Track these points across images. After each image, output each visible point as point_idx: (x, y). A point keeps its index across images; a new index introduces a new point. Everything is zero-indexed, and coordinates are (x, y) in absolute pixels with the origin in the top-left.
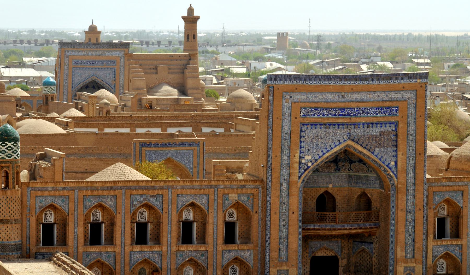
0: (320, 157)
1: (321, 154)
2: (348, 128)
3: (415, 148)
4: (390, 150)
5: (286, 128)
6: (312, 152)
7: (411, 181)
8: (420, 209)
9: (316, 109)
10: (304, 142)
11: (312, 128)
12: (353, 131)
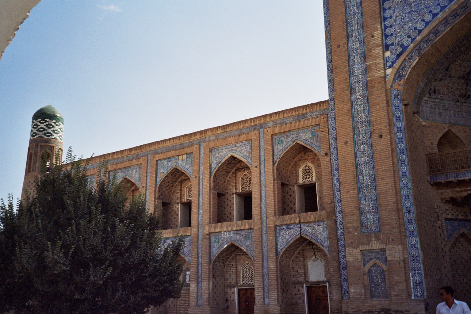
6: (410, 20)
10: (390, 8)
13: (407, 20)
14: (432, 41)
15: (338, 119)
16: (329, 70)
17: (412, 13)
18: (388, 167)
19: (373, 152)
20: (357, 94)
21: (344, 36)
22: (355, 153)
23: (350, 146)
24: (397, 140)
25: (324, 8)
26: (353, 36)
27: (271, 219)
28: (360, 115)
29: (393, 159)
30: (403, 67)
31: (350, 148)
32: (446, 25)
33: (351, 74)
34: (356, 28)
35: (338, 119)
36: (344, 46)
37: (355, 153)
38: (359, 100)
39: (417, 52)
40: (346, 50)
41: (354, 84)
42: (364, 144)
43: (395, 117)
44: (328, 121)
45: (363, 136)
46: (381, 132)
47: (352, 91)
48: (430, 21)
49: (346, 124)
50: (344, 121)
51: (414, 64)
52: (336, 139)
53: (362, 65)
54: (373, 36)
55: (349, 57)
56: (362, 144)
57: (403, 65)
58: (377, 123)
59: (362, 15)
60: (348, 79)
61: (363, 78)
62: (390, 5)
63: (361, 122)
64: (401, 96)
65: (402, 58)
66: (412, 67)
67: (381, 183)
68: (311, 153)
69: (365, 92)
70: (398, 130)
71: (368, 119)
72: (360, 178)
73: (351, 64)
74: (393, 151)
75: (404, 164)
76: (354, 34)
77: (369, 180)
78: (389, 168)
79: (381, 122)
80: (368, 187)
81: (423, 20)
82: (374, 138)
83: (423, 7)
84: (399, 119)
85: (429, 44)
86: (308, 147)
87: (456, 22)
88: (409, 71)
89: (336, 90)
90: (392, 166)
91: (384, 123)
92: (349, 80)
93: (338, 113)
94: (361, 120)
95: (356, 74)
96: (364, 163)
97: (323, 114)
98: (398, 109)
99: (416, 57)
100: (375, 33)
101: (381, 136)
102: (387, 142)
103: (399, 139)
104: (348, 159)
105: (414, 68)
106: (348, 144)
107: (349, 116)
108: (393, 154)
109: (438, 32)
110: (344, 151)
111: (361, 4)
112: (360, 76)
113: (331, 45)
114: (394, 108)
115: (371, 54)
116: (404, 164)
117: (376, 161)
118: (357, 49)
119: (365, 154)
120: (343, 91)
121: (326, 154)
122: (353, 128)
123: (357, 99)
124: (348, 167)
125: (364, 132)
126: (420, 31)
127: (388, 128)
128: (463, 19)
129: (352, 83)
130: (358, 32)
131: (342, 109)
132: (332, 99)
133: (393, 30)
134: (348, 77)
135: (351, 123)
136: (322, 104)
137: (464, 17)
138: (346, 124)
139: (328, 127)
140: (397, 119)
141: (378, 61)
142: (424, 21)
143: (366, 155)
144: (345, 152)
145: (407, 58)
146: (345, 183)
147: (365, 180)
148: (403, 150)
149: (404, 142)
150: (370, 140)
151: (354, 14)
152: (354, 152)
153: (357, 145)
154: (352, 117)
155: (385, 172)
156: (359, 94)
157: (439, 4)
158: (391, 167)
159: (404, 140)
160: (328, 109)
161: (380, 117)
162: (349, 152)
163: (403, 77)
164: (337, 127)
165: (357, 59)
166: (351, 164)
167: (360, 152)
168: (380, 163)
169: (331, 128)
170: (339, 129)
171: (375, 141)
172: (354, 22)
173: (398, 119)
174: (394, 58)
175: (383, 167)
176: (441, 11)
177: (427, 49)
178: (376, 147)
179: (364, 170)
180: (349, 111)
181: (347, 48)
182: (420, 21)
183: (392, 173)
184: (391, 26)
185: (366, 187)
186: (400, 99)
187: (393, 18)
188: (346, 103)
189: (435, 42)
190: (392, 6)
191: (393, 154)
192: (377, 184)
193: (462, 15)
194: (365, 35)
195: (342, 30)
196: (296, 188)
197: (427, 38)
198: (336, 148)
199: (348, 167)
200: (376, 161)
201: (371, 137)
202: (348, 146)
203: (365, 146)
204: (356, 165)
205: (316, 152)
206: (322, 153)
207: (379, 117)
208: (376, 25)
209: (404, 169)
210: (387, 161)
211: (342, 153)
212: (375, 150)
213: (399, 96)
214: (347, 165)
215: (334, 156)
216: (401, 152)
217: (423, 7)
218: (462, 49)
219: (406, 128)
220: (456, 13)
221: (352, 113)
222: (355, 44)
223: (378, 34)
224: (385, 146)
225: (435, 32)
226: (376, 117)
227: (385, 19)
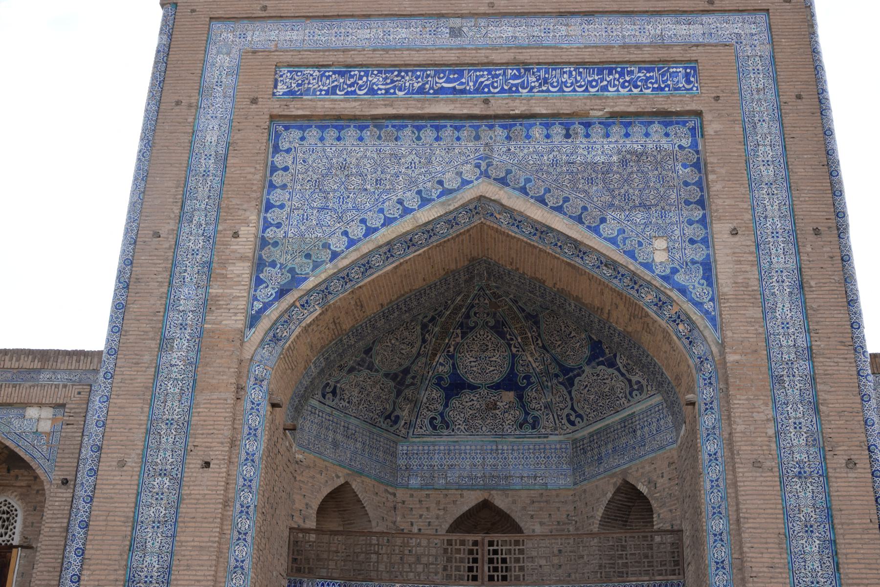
0: (352, 243)
1: (357, 231)
2: (477, 138)
3: (792, 210)
4: (673, 217)
5: (212, 137)
7: (788, 343)
8: (851, 464)
9: (341, 74)
10: (284, 187)
11: (322, 139)
13: (314, 222)
14: (352, 283)
15: (115, 401)
16: (122, 280)
17: (326, 211)
18: (207, 542)
19: (180, 499)
20: (174, 355)
21: (172, 216)
22: (138, 494)
23: (131, 473)
24: (241, 482)
25: (142, 140)
26: (192, 222)
28: (169, 403)
29: (222, 524)
30: (286, 318)
31: (129, 478)
32: (388, 258)
33: (169, 304)
34: (203, 206)
35: (115, 401)
36: (167, 238)
37: (138, 494)
38: (174, 369)
39: (320, 295)
40: (170, 248)
41: (173, 330)
42: (165, 474)
43: (246, 427)
44: (88, 401)
45: (165, 457)
46: (209, 455)
47: (164, 344)
48: (359, 240)
49: (132, 418)
50: (130, 409)
51: (309, 320)
52: (100, 448)
53: (200, 291)
54: (236, 235)
55: (174, 265)
56: (160, 475)
57: (286, 316)
58: (205, 432)
59: (222, 182)
60: (162, 314)
61: (195, 322)
62: (285, 182)
63: (169, 423)
64: (269, 384)
65: (289, 299)
66: (303, 324)
67: (182, 577)
68: (26, 473)
69: (192, 354)
70: (247, 459)
71: (186, 419)
72: (137, 555)
73: (176, 281)
74: (226, 504)
75: (245, 540)
76: (196, 218)
77: (157, 566)
78: (209, 544)
79: (216, 432)
80: (151, 582)
82: (191, 466)
83: (350, 205)
84: (255, 435)
85: (348, 286)
86: (22, 454)
87: (408, 258)
88: (296, 333)
89: (126, 331)
90: (217, 539)
91: (220, 436)
92: (164, 316)
93: (120, 387)
94: (170, 418)
95: (181, 308)
96: (154, 522)
97: (80, 382)
98: (257, 410)
99: (317, 307)
100: (242, 228)
101: (207, 464)
102: (218, 481)
103: (245, 480)
104: (117, 505)
105: (306, 329)
106: (125, 468)
107: (144, 399)
108: (225, 513)
109: (370, 267)
110: (113, 482)
111: (226, 159)
112: (190, 314)
113: (138, 226)
114: (249, 406)
115: (224, 272)
116: (245, 540)
117: (184, 522)
118: (195, 253)
119: (162, 499)
120: (144, 339)
121: (65, 482)
122: (148, 432)
123: (172, 365)
124: (113, 523)
125: (169, 447)
126: (335, 255)
127: (227, 449)
128: (420, 255)
129: (168, 326)
130: (206, 216)
131: (131, 380)
132: (112, 350)
133: (280, 234)
134: (162, 310)
135: (146, 418)
136: (82, 358)
137: (424, 252)
138: (132, 418)
139: (85, 416)
140: (250, 434)
141: (236, 293)
142: (347, 236)
143: (163, 502)
144: (114, 485)
145: (298, 304)
146: (97, 564)
147: (146, 564)
148: (248, 507)
149: (254, 489)
150: (180, 469)
151: (206, 174)
152: (137, 490)
153: (146, 475)
154: (151, 406)
155: (197, 553)
156: (179, 354)
157: (381, 211)
158: (215, 542)
159: (254, 484)
160: (96, 371)
161: (215, 419)
162: (123, 487)
163: (281, 343)
164: (108, 422)
165: (190, 271)
166: (123, 519)
167: (150, 492)
168: (191, 529)
169: (92, 419)
170: (114, 426)
171: (190, 474)
172: (203, 192)
173: (253, 433)
174: (272, 295)
175: (196, 539)
176: (383, 225)
177: (341, 296)
178: (192, 488)
179: (149, 539)
180: (146, 388)
181: (173, 243)
183: (214, 557)
184: (278, 226)
185: (146, 582)
186: (265, 387)
187: (286, 208)
188: (144, 369)
189: (360, 287)
190: (289, 185)
191: (225, 513)
192: (173, 577)
193: (421, 246)
194: (220, 228)
195: (171, 200)
197: (346, 272)
198: (94, 472)
199: (113, 523)
200: (184, 522)
202: (123, 473)
203: (166, 481)
204: (135, 523)
205: (39, 472)
206: (56, 476)
207: (211, 418)
208: (248, 213)
209: (242, 552)
210: (207, 525)
211: (107, 487)
212: (187, 494)
213: (265, 383)
214: (113, 518)
215: (85, 491)
216: (242, 512)
217: (350, 205)
218: (405, 316)
219: (265, 458)
220: (411, 240)
221: (153, 395)
222: (193, 241)
223: (249, 232)
224: (212, 490)
225: (365, 265)
226: (207, 418)
227: (269, 206)
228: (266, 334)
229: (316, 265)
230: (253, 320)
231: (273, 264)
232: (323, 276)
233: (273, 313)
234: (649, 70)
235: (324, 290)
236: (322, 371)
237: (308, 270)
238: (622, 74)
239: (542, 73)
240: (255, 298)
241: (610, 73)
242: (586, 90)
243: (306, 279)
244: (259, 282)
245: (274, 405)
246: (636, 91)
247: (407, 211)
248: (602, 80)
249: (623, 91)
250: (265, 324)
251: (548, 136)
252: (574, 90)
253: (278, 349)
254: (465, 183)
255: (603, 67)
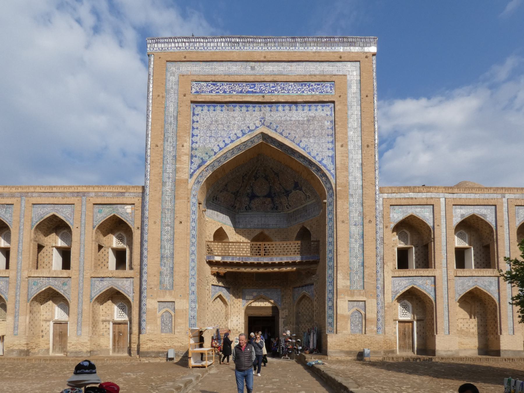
0: (221, 149)
1: (222, 145)
12: (268, 114)
27: (88, 271)
30: (201, 175)
33: (164, 171)
45: (168, 220)
47: (164, 184)
63: (168, 210)
65: (202, 168)
81: (218, 146)
122: (162, 212)
125: (169, 217)
126: (215, 153)
154: (162, 204)
157: (230, 137)
182: (216, 146)
196: (110, 251)
201: (174, 222)
203: (169, 227)
221: (162, 201)
225: (225, 156)
228: (195, 180)
229: (210, 157)
230: (191, 175)
231: (196, 156)
232: (212, 161)
233: (197, 173)
234: (318, 85)
235: (212, 165)
236: (213, 192)
237: (207, 159)
238: (309, 86)
239: (282, 85)
240: (191, 168)
241: (305, 86)
242: (297, 92)
243: (206, 162)
244: (192, 163)
245: (200, 204)
246: (313, 93)
247: (238, 138)
248: (302, 88)
249: (309, 93)
250: (195, 177)
251: (284, 110)
252: (293, 92)
253: (199, 185)
254: (257, 127)
255: (303, 83)
